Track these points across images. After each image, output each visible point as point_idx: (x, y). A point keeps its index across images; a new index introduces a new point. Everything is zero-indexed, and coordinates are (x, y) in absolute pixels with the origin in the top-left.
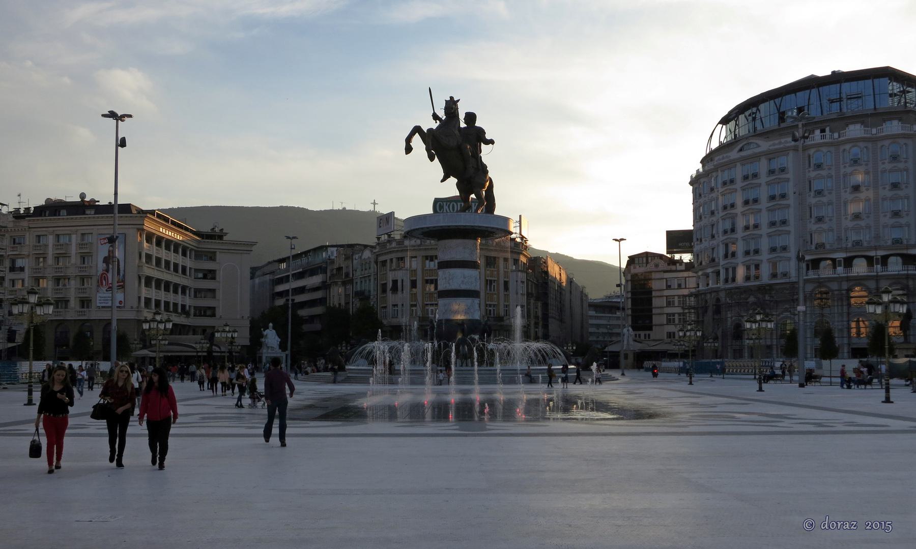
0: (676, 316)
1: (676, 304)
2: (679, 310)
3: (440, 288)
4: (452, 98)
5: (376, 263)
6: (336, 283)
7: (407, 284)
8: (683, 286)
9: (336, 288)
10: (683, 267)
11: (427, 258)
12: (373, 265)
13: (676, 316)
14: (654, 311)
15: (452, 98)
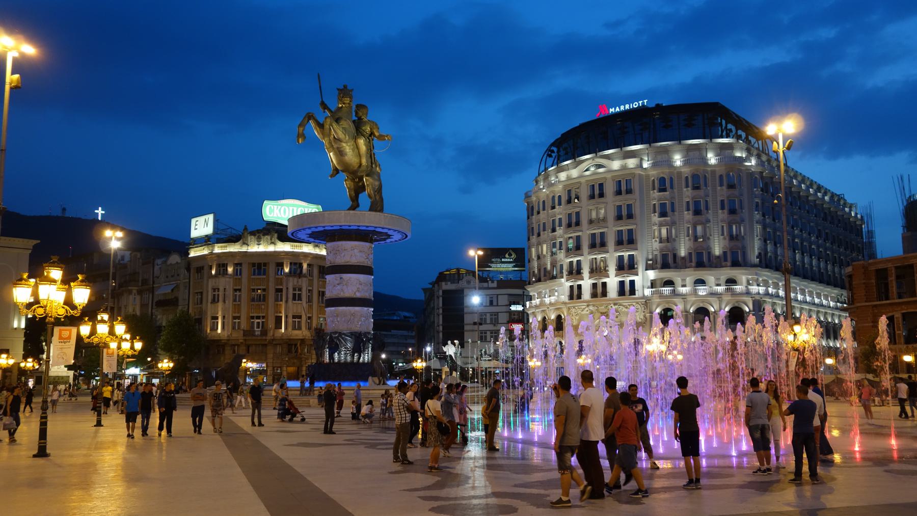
0: (488, 333)
1: (488, 321)
2: (491, 327)
3: (328, 295)
4: (345, 87)
5: (188, 269)
6: (130, 292)
7: (230, 293)
8: (495, 303)
9: (131, 297)
10: (495, 285)
11: (254, 265)
12: (183, 272)
13: (488, 334)
14: (466, 328)
15: (345, 87)
